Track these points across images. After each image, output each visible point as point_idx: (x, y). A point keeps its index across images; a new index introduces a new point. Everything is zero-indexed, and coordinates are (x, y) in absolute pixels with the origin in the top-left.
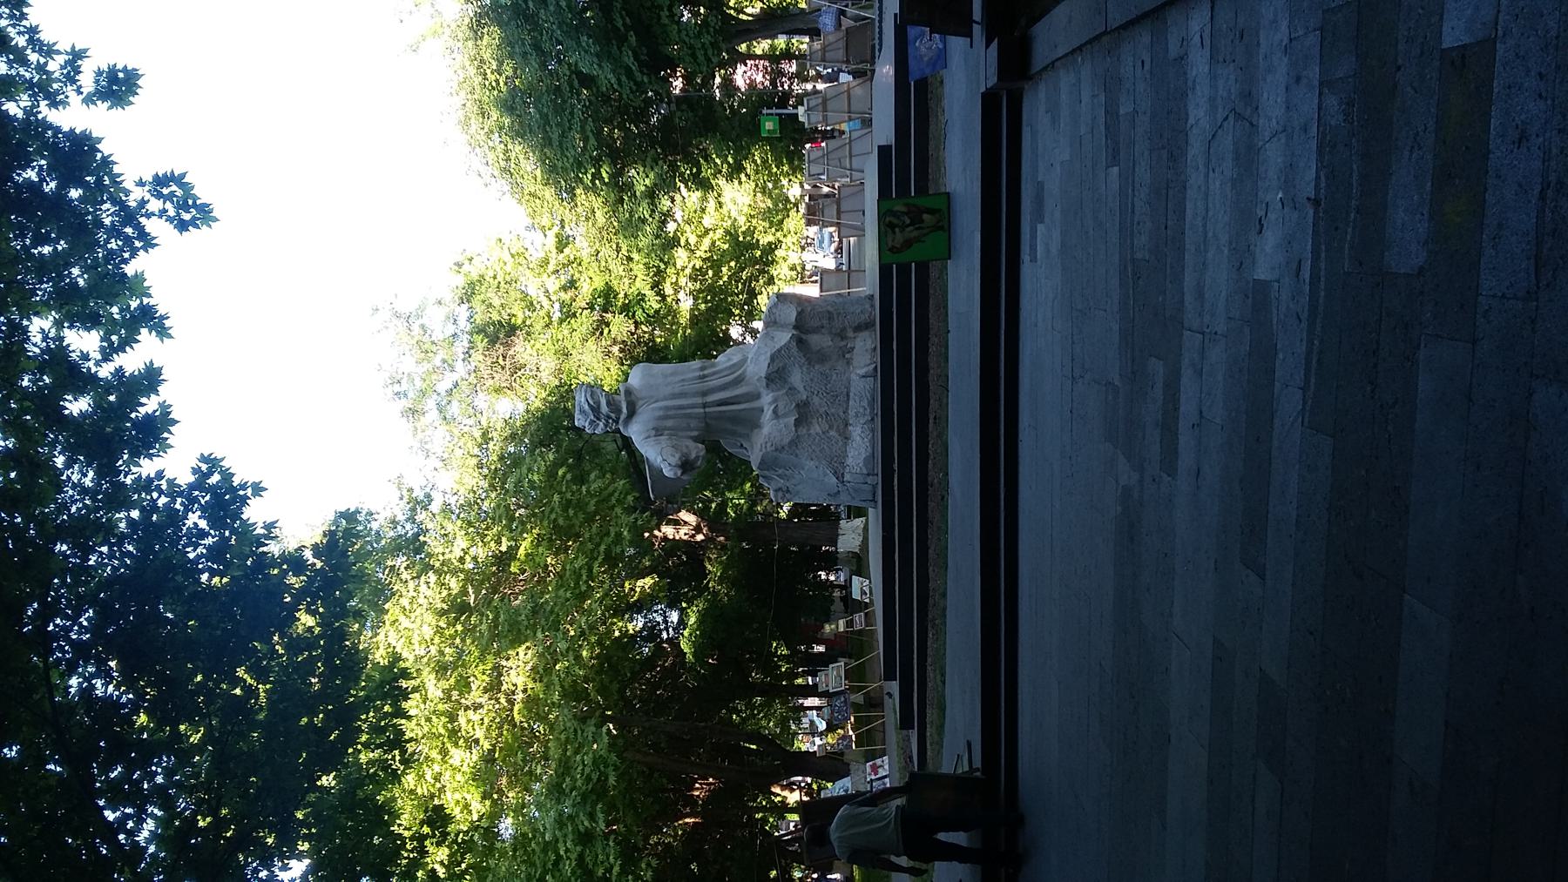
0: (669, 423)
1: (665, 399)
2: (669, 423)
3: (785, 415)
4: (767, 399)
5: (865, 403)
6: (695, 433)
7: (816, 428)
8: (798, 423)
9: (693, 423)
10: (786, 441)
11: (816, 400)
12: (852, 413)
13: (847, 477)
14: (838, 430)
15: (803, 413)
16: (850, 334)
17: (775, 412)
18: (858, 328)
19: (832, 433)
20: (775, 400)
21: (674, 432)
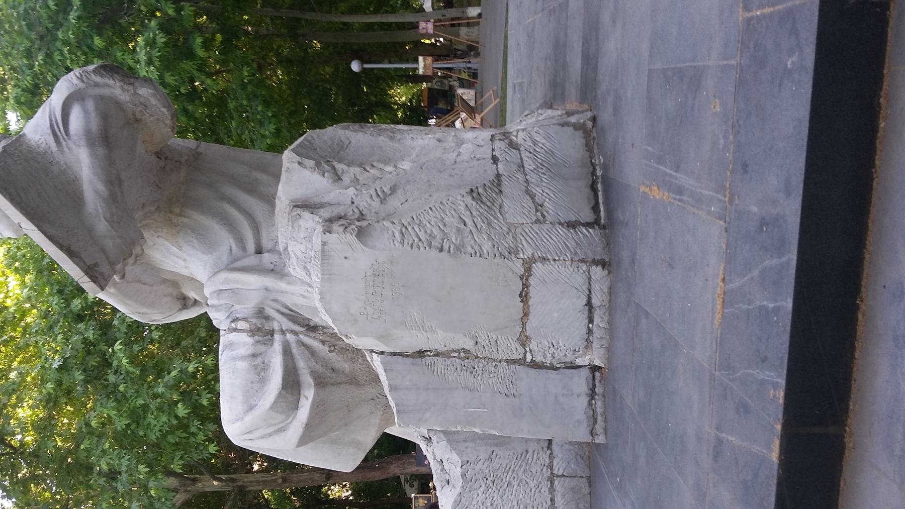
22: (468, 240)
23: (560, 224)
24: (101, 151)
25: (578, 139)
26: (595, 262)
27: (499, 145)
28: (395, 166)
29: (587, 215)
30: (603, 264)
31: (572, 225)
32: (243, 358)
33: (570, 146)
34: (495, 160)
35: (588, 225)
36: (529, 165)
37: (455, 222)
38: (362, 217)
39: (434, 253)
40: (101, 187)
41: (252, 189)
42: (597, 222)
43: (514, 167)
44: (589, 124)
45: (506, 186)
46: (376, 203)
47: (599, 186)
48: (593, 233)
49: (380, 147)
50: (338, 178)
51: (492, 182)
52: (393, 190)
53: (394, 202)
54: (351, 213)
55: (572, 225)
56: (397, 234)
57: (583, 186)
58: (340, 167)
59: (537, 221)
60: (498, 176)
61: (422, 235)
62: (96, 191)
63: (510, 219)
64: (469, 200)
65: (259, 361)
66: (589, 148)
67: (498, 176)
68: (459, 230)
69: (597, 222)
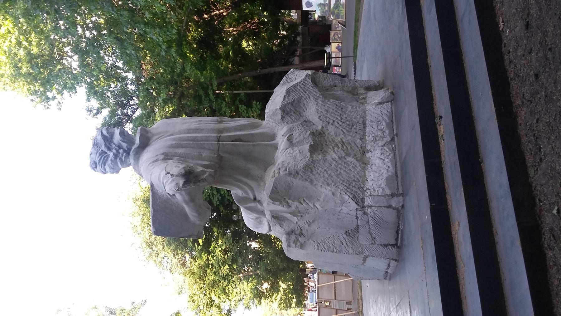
0: (181, 151)
1: (180, 133)
2: (181, 151)
3: (301, 143)
4: (281, 132)
5: (384, 126)
6: (207, 163)
7: (332, 155)
8: (313, 149)
9: (205, 154)
10: (301, 165)
11: (331, 129)
12: (369, 138)
13: (368, 201)
14: (355, 157)
15: (318, 143)
16: (362, 91)
17: (290, 139)
18: (369, 89)
19: (350, 159)
20: (290, 130)
21: (182, 158)
22: (344, 250)
23: (381, 245)
24: (192, 204)
25: (394, 213)
26: (393, 259)
27: (359, 213)
28: (314, 205)
29: (393, 242)
30: (396, 260)
31: (386, 246)
32: (253, 219)
33: (390, 216)
34: (357, 218)
35: (393, 245)
36: (371, 222)
37: (339, 243)
38: (301, 234)
39: (330, 253)
40: (194, 214)
41: (248, 175)
42: (396, 244)
43: (365, 223)
44: (400, 208)
45: (361, 230)
46: (307, 226)
47: (400, 232)
48: (394, 250)
49: (307, 188)
50: (290, 206)
51: (355, 229)
52: (313, 221)
53: (314, 227)
54: (296, 229)
55: (386, 246)
56: (316, 246)
57: (393, 231)
58: (290, 202)
59: (372, 244)
60: (358, 225)
61: (325, 246)
62: (193, 216)
63: (361, 242)
64: (345, 236)
65: (258, 220)
66: (398, 217)
67: (358, 225)
68: (340, 246)
69: (396, 244)
